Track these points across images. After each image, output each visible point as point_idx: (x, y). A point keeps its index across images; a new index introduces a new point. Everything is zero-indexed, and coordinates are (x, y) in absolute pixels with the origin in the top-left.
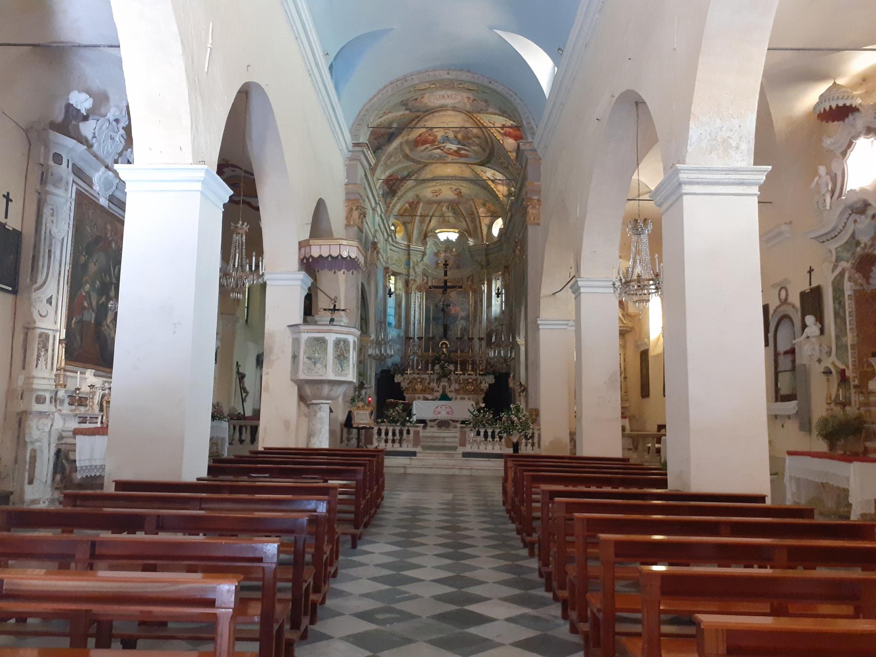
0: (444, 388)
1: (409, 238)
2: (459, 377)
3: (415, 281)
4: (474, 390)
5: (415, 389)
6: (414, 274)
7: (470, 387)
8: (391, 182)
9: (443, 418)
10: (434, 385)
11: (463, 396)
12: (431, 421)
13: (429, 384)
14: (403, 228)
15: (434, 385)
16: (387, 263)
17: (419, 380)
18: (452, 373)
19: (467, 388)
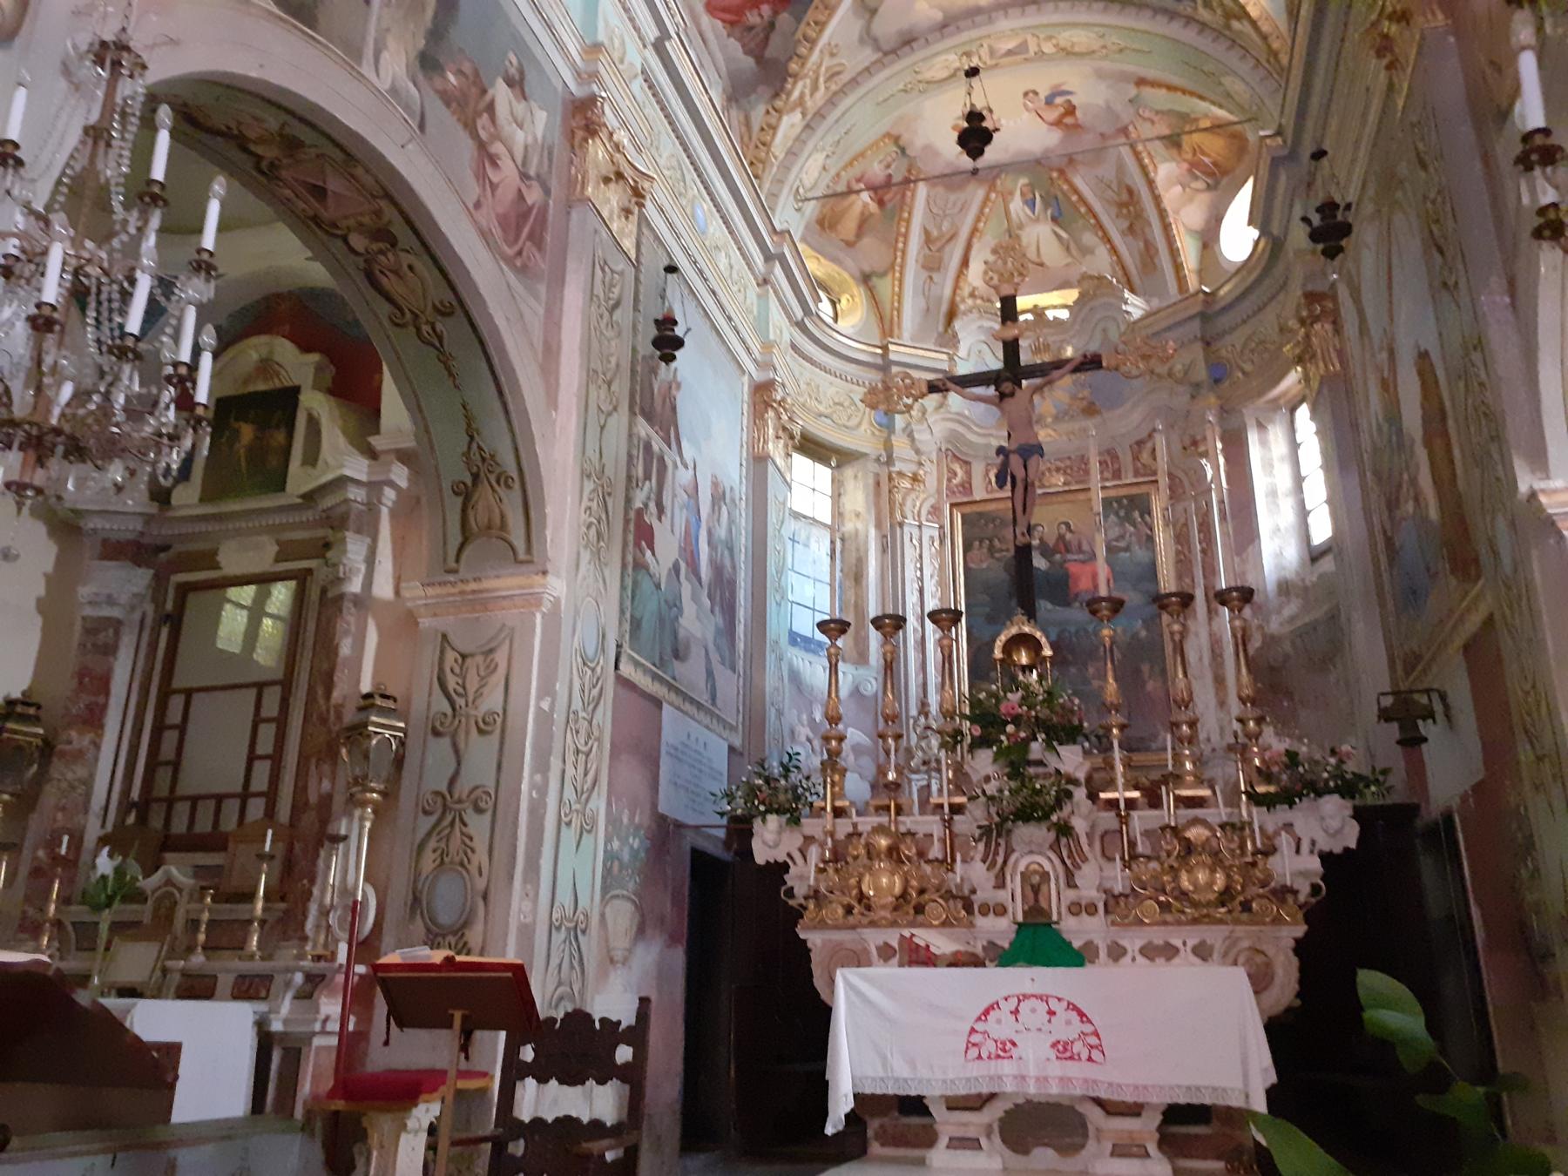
0: (1035, 886)
1: (886, 324)
2: (1124, 820)
3: (915, 479)
4: (1226, 896)
5: (861, 897)
6: (916, 458)
7: (1201, 879)
8: (752, 18)
9: (1032, 1089)
10: (973, 873)
11: (1157, 935)
12: (956, 1104)
13: (947, 863)
14: (859, 293)
15: (973, 873)
16: (766, 365)
17: (883, 842)
18: (1080, 794)
19: (1185, 883)
